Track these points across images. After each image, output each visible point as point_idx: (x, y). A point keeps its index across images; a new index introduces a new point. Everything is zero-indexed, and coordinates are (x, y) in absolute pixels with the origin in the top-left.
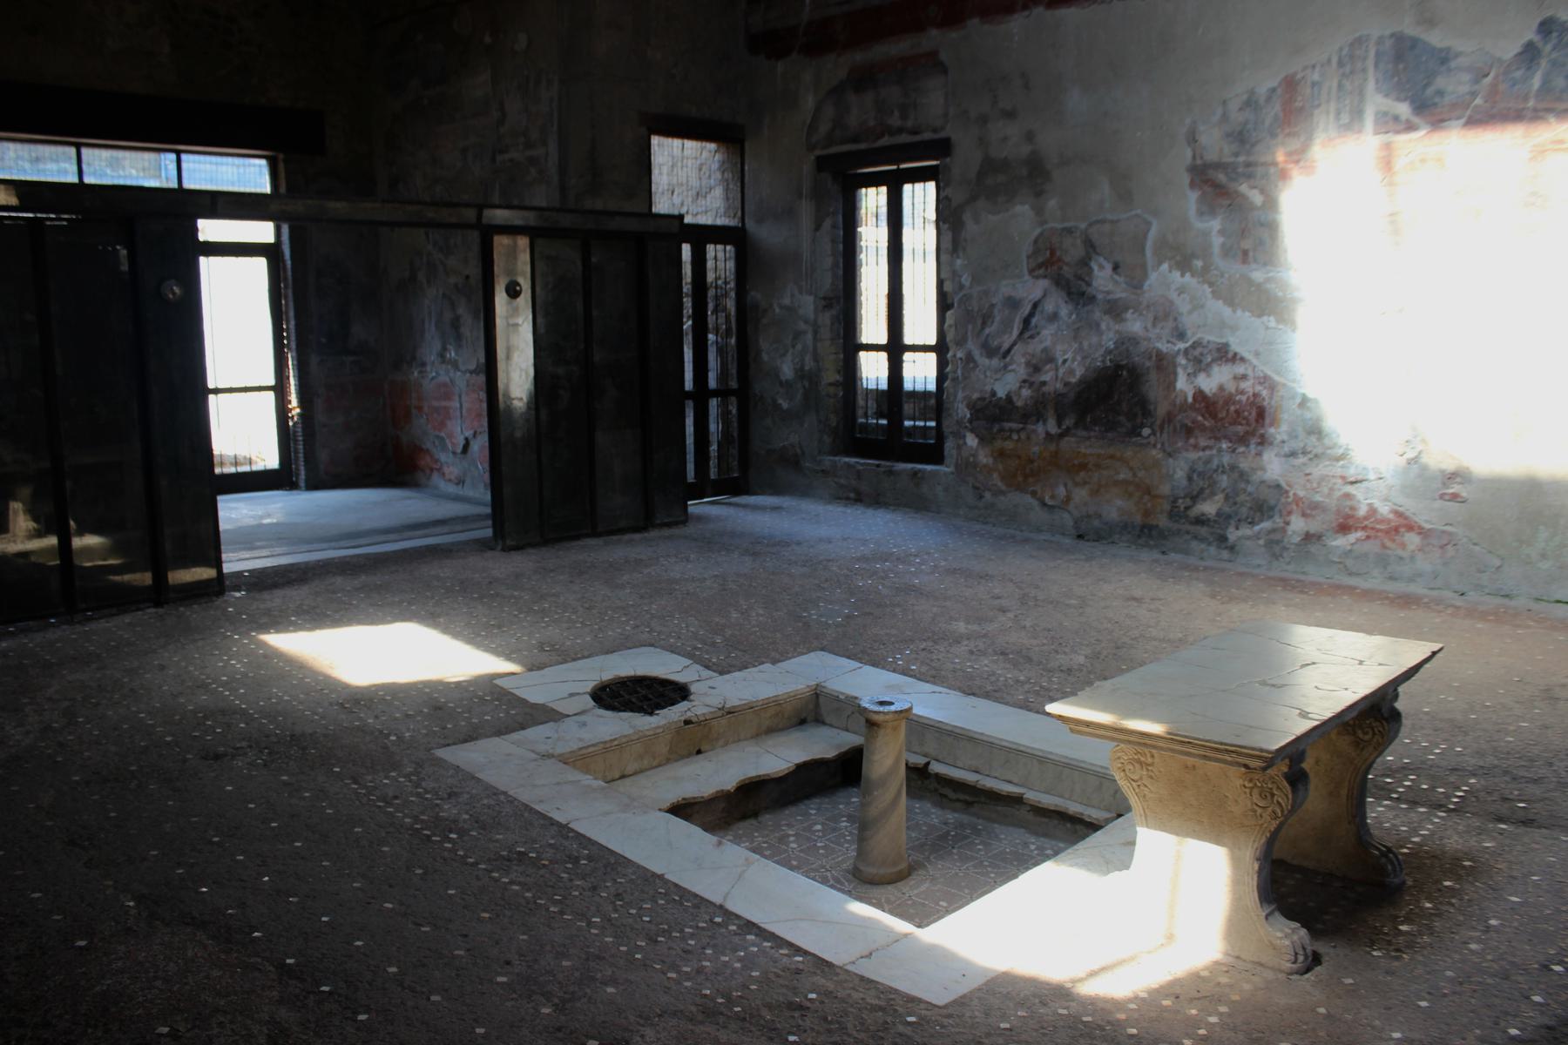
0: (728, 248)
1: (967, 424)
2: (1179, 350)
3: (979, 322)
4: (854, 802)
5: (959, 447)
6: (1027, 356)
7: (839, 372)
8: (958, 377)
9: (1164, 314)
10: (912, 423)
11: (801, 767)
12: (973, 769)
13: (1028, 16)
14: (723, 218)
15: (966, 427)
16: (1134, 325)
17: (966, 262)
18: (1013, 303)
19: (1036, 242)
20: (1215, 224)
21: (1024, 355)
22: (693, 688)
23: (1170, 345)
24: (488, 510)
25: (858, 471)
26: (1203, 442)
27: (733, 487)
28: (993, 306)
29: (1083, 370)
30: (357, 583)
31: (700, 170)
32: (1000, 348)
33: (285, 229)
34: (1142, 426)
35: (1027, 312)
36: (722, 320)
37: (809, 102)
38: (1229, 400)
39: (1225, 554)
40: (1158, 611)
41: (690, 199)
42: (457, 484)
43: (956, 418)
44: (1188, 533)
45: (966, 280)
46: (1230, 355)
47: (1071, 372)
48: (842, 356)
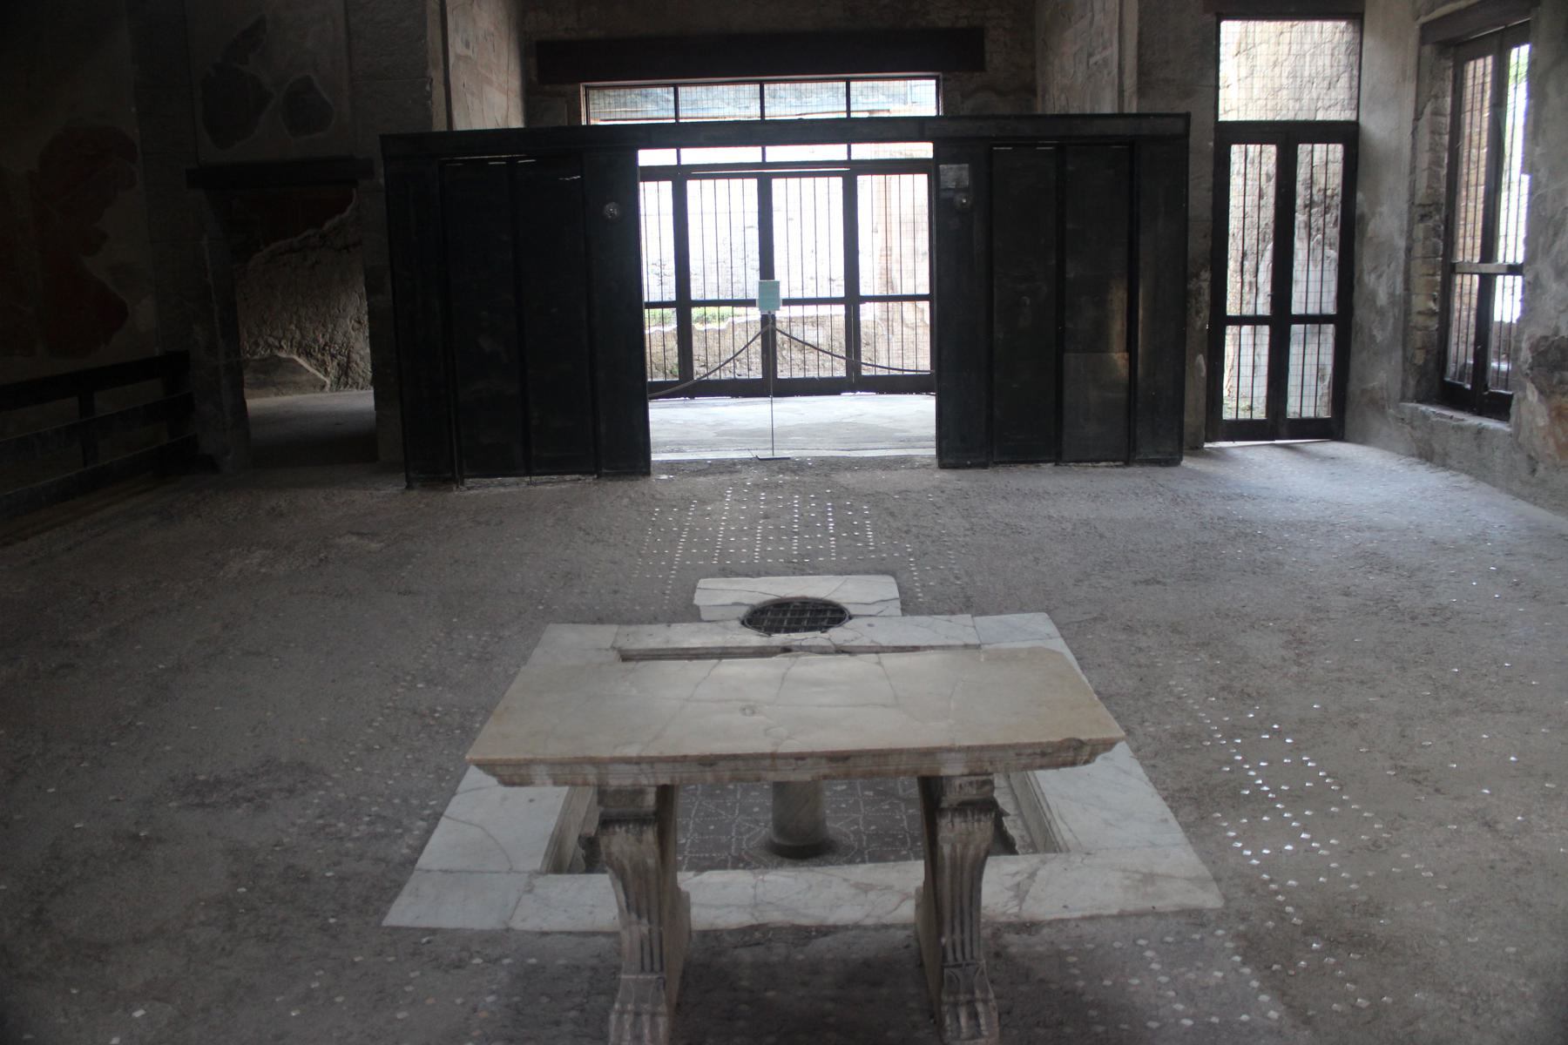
1: (1529, 372)
7: (1435, 300)
48: (1439, 278)
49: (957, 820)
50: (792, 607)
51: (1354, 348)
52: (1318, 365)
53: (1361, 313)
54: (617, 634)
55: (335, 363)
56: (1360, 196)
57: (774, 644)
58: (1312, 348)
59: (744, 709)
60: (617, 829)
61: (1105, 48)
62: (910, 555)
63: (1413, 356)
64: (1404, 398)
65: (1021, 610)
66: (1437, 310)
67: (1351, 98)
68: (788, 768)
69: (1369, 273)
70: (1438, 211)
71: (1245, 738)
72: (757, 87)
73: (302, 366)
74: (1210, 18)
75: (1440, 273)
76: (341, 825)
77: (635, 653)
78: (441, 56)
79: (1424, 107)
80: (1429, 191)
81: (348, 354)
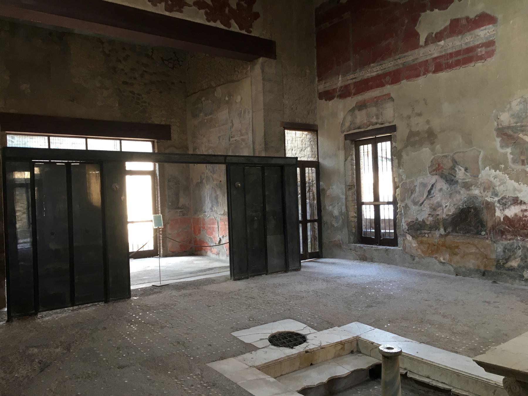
0: (313, 169)
2: (496, 200)
3: (410, 192)
4: (376, 388)
5: (404, 240)
6: (430, 205)
7: (355, 213)
8: (402, 213)
9: (489, 187)
10: (384, 231)
11: (353, 372)
12: (427, 376)
13: (425, 77)
14: (311, 158)
15: (406, 232)
16: (476, 192)
17: (404, 170)
18: (424, 185)
19: (432, 161)
20: (509, 150)
21: (429, 205)
22: (308, 337)
23: (491, 199)
24: (229, 265)
25: (364, 250)
26: (509, 237)
27: (317, 255)
28: (415, 186)
29: (454, 210)
30: (180, 293)
31: (302, 141)
32: (419, 202)
33: (157, 164)
34: (481, 231)
35: (429, 188)
36: (311, 195)
37: (341, 115)
38: (520, 219)
39: (523, 283)
40: (498, 307)
41: (299, 152)
42: (217, 255)
43: (402, 229)
44: (505, 274)
45: (404, 177)
46: (519, 202)
47: (449, 210)
48: (356, 207)
51: (324, 229)
53: (325, 218)
61: (242, 135)
63: (352, 230)
69: (329, 206)
72: (84, 140)
77: (260, 367)
79: (348, 158)
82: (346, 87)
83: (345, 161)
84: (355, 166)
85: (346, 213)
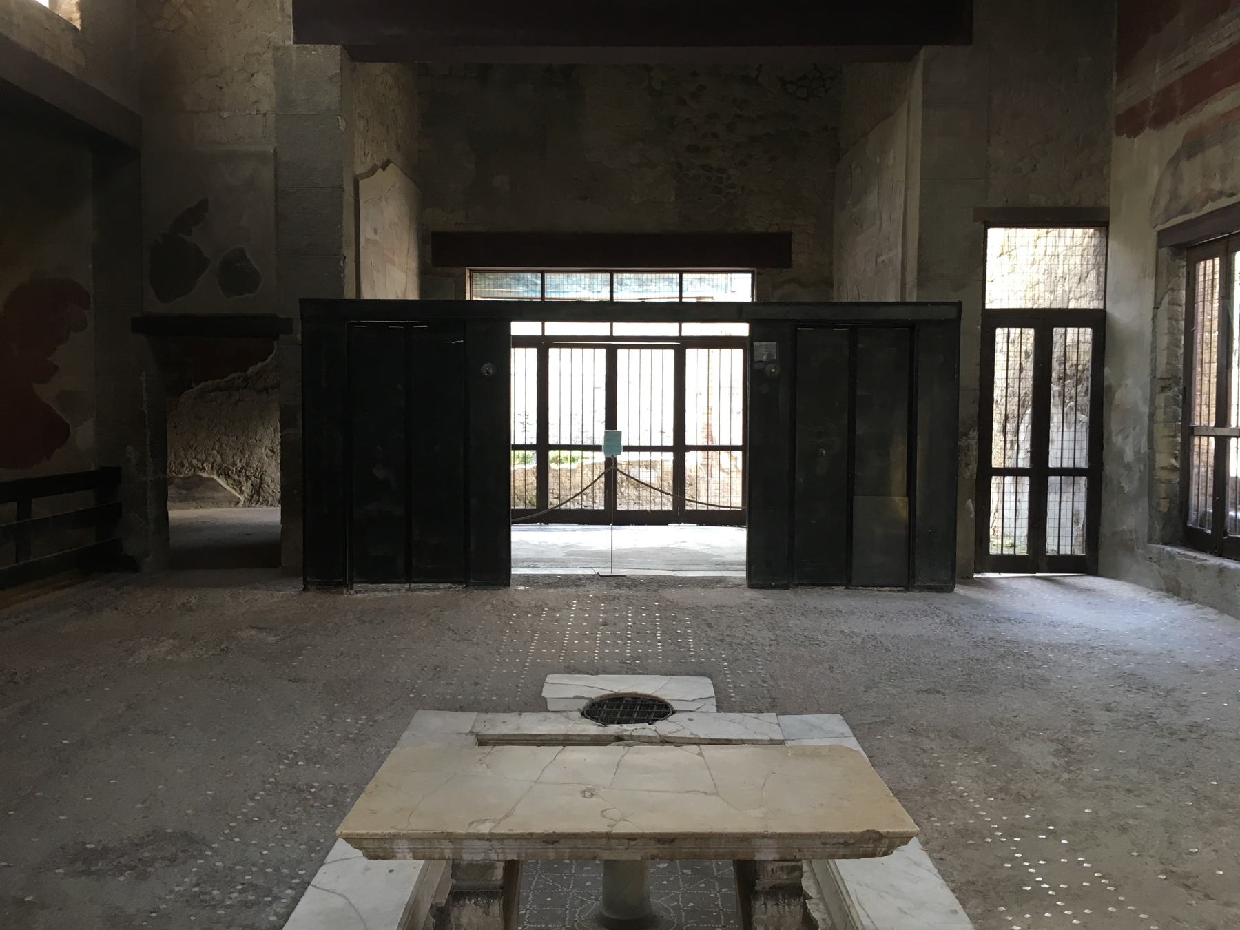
7: (1176, 458)
48: (1179, 439)
49: (770, 904)
50: (624, 702)
51: (1105, 496)
52: (1073, 510)
53: (1109, 468)
54: (475, 720)
55: (250, 483)
56: (1107, 370)
57: (609, 733)
58: (1067, 496)
59: (584, 792)
60: (468, 902)
61: (890, 250)
62: (725, 660)
63: (1158, 504)
64: (1150, 540)
65: (819, 711)
66: (1178, 466)
67: (1099, 291)
68: (620, 847)
69: (1117, 435)
70: (1177, 384)
71: (1023, 836)
73: (220, 485)
74: (980, 225)
75: (1180, 435)
76: (215, 892)
77: (490, 738)
78: (353, 240)
80: (1169, 367)
81: (261, 476)
82: (1167, 91)
83: (1154, 308)
84: (1183, 323)
85: (1149, 456)
